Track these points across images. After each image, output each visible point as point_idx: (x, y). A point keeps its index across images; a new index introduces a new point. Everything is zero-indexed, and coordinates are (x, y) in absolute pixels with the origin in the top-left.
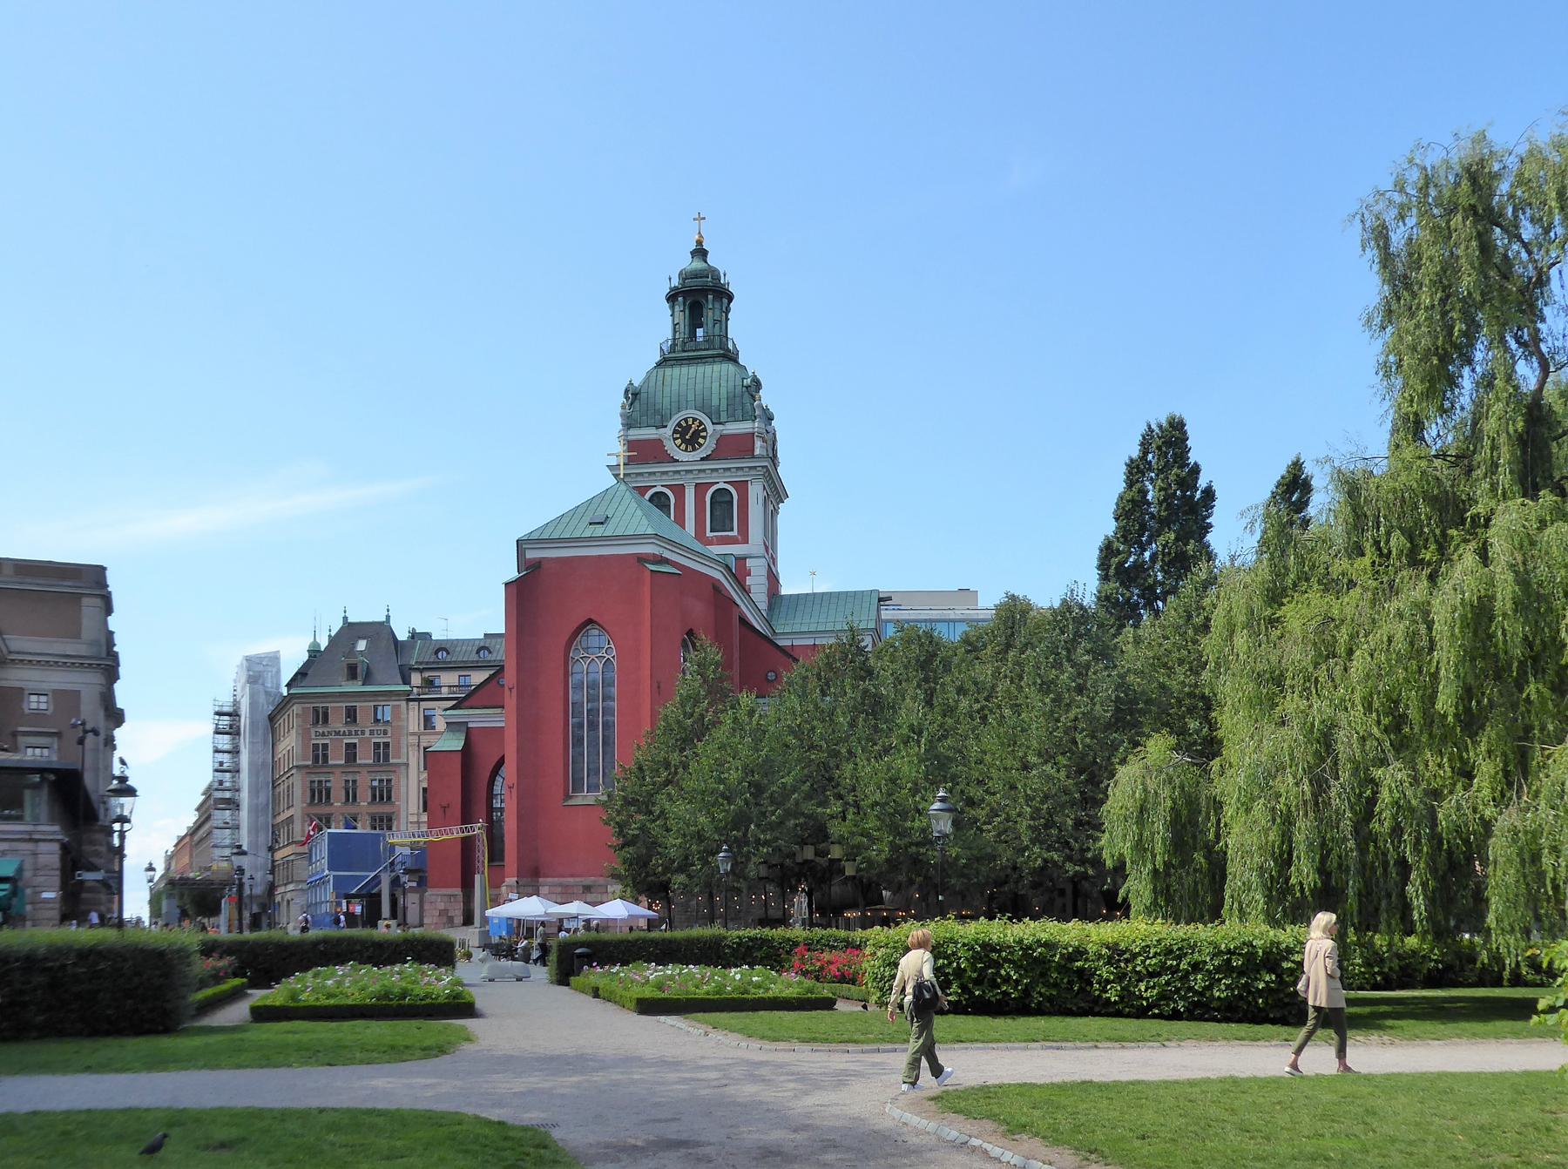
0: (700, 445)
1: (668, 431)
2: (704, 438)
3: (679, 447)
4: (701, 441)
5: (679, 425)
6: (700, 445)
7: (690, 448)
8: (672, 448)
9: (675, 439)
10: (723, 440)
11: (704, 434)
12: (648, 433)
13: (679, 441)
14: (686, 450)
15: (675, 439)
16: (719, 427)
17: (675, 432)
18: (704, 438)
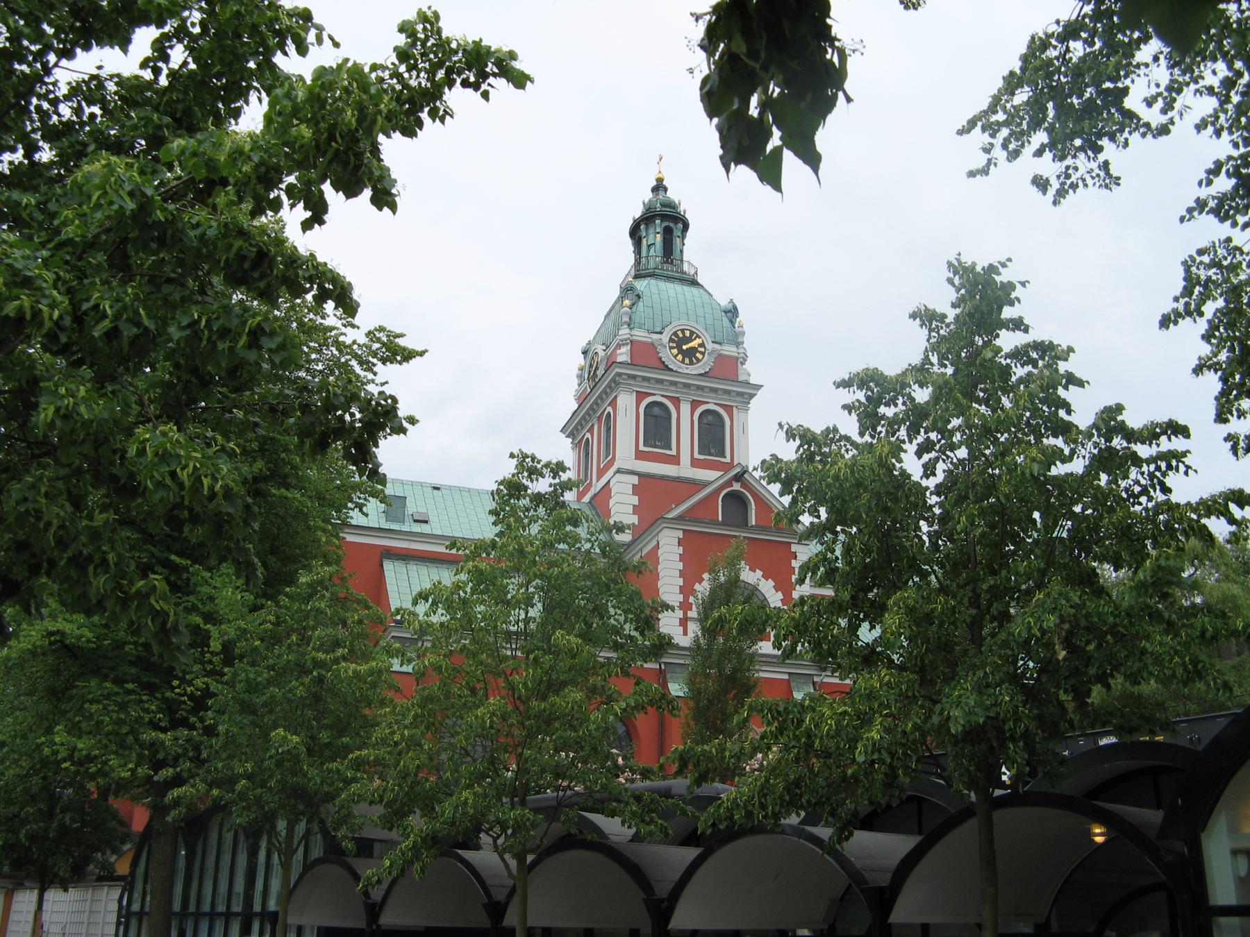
0: (698, 360)
1: (665, 338)
2: (703, 354)
3: (675, 357)
4: (698, 355)
5: (675, 334)
6: (698, 360)
7: (687, 361)
8: (669, 356)
9: (671, 348)
10: (720, 359)
11: (702, 350)
12: (640, 335)
13: (675, 351)
14: (683, 362)
15: (671, 348)
16: (717, 347)
17: (671, 340)
18: (703, 354)
